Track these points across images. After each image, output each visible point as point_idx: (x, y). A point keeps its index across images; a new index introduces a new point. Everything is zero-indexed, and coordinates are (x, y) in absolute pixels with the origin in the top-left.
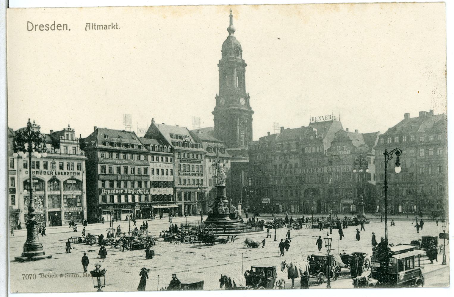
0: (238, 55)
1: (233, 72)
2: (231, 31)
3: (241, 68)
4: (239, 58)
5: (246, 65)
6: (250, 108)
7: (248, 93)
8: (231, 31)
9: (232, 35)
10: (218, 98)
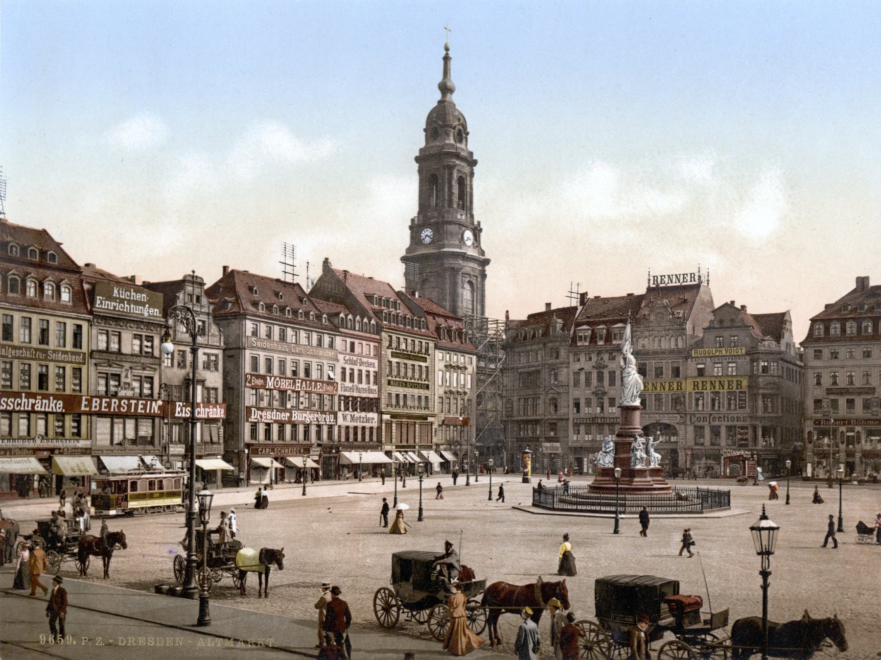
0: (461, 141)
1: (451, 174)
2: (445, 89)
3: (467, 170)
4: (463, 146)
5: (475, 163)
6: (483, 253)
7: (479, 223)
8: (445, 89)
9: (449, 97)
10: (415, 228)
